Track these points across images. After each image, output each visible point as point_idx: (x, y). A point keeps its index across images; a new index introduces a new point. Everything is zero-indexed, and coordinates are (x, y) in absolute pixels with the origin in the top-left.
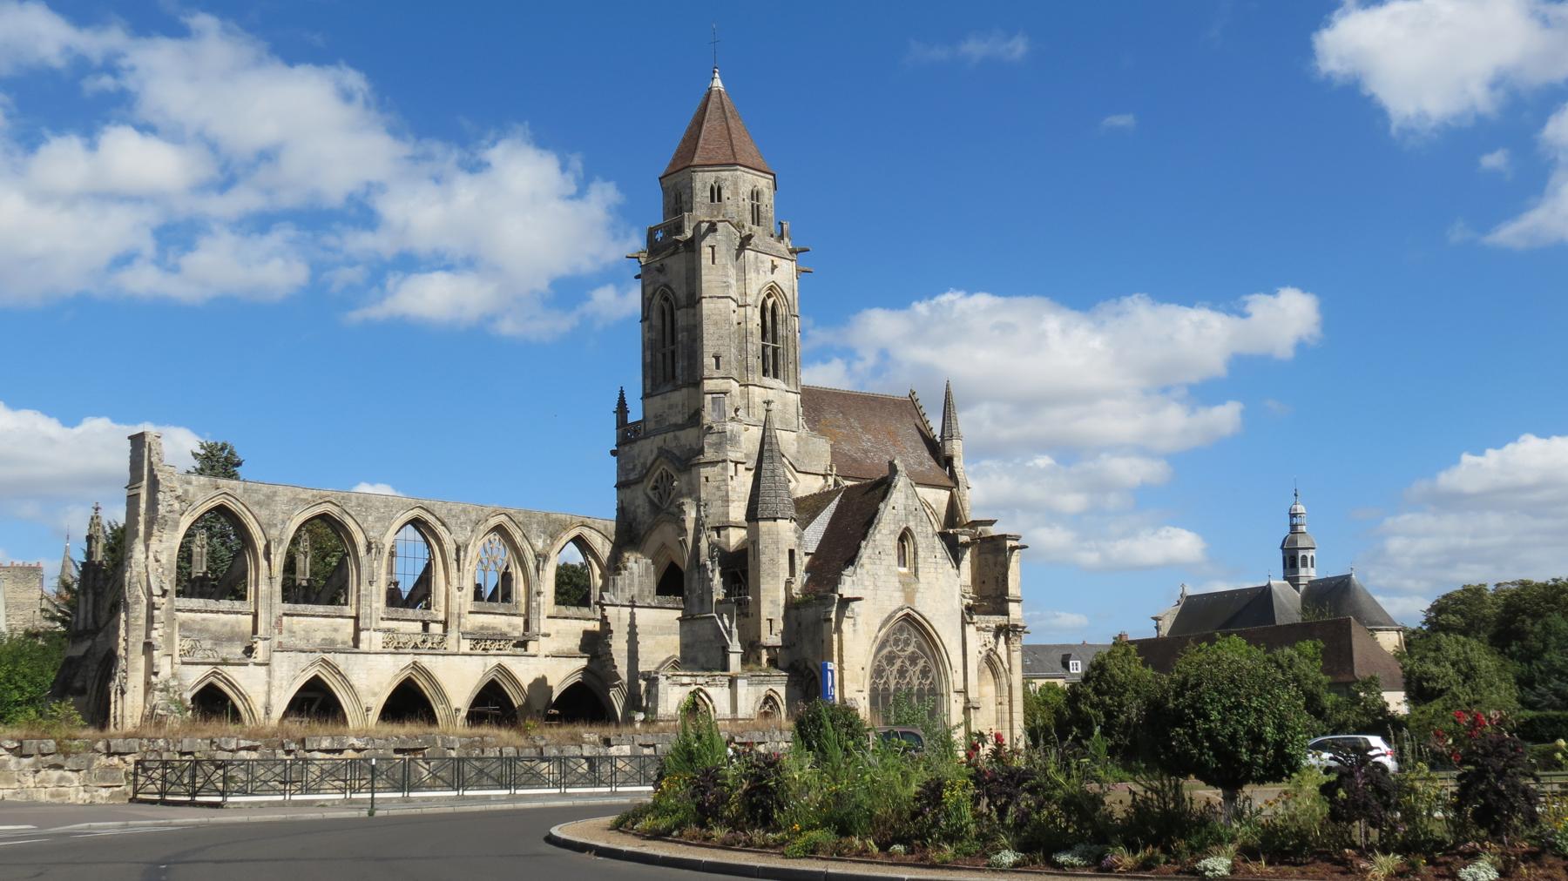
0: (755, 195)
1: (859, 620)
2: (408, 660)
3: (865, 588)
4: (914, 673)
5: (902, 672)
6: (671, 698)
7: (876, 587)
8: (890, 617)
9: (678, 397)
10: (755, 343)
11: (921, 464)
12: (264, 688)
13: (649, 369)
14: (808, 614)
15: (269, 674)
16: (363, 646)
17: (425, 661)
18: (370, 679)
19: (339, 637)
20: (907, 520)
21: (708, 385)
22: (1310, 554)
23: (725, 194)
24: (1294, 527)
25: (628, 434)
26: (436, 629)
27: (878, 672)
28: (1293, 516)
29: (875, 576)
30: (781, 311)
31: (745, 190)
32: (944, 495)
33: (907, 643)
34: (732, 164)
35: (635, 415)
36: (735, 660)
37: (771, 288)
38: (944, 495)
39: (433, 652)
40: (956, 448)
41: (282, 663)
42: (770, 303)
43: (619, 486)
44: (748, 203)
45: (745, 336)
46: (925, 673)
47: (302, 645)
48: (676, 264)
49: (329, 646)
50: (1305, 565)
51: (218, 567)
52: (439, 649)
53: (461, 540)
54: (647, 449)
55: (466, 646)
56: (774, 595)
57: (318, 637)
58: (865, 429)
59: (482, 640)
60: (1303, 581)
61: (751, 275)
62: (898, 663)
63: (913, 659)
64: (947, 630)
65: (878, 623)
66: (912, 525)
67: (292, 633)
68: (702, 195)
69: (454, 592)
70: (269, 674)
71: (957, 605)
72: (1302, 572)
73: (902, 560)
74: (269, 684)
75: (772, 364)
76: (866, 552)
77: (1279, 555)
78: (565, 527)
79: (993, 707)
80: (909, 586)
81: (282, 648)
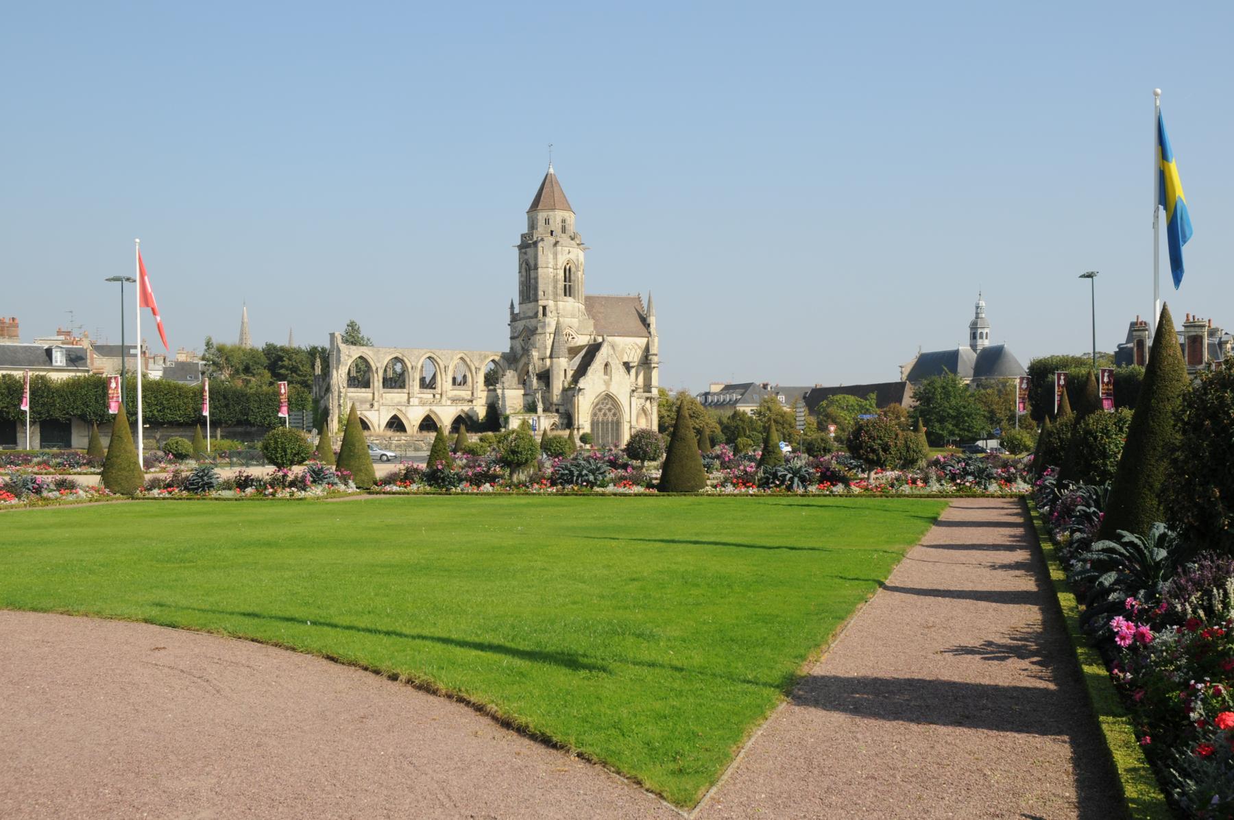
0: (564, 221)
2: (427, 408)
4: (610, 415)
5: (605, 414)
6: (514, 424)
9: (532, 305)
10: (561, 284)
13: (521, 293)
14: (570, 393)
17: (435, 408)
18: (413, 418)
21: (541, 303)
22: (985, 331)
24: (977, 313)
25: (514, 318)
26: (438, 396)
27: (595, 415)
28: (977, 308)
30: (573, 269)
31: (559, 220)
32: (645, 340)
34: (553, 209)
35: (516, 311)
36: (540, 409)
38: (645, 340)
39: (437, 405)
40: (652, 320)
43: (512, 338)
45: (556, 281)
46: (614, 415)
48: (530, 251)
49: (399, 404)
50: (981, 337)
51: (361, 377)
52: (439, 403)
54: (520, 325)
55: (449, 402)
56: (558, 384)
57: (396, 401)
59: (455, 400)
60: (979, 348)
61: (559, 256)
63: (610, 410)
64: (623, 399)
68: (541, 222)
69: (444, 383)
72: (979, 342)
73: (606, 373)
75: (568, 291)
76: (591, 370)
77: (968, 332)
78: (486, 357)
80: (607, 384)
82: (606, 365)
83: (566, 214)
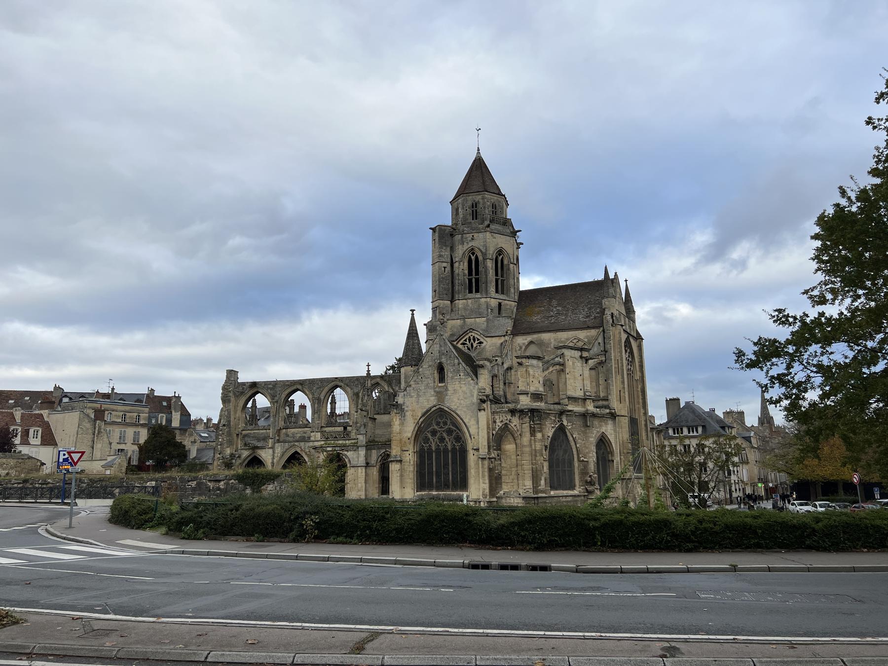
0: (475, 205)
1: (407, 414)
3: (412, 397)
7: (418, 396)
8: (427, 411)
11: (587, 317)
12: (270, 457)
15: (274, 452)
16: (312, 439)
19: (306, 435)
20: (440, 358)
23: (460, 210)
29: (418, 391)
30: (480, 258)
32: (593, 332)
33: (445, 423)
37: (472, 249)
41: (279, 449)
42: (473, 258)
44: (469, 211)
47: (291, 439)
53: (356, 391)
57: (299, 435)
58: (559, 305)
62: (438, 434)
65: (420, 415)
66: (444, 360)
67: (288, 436)
70: (274, 452)
71: (475, 400)
73: (442, 379)
74: (273, 455)
79: (514, 457)
81: (279, 441)
82: (441, 369)
83: (478, 198)
